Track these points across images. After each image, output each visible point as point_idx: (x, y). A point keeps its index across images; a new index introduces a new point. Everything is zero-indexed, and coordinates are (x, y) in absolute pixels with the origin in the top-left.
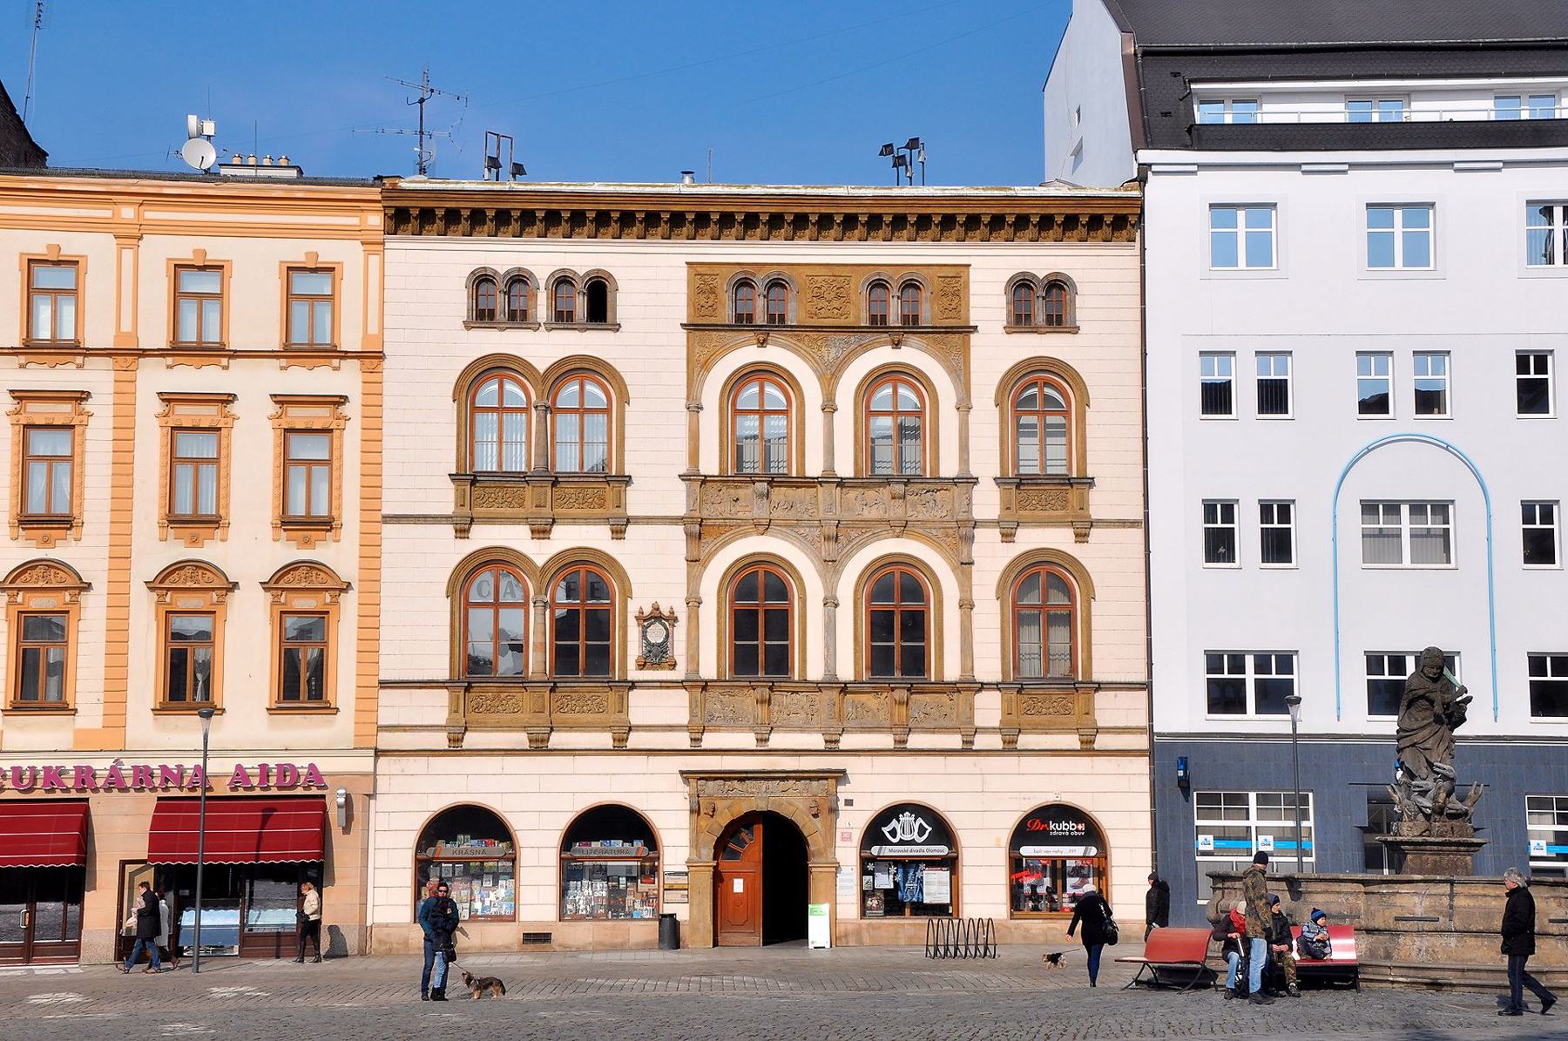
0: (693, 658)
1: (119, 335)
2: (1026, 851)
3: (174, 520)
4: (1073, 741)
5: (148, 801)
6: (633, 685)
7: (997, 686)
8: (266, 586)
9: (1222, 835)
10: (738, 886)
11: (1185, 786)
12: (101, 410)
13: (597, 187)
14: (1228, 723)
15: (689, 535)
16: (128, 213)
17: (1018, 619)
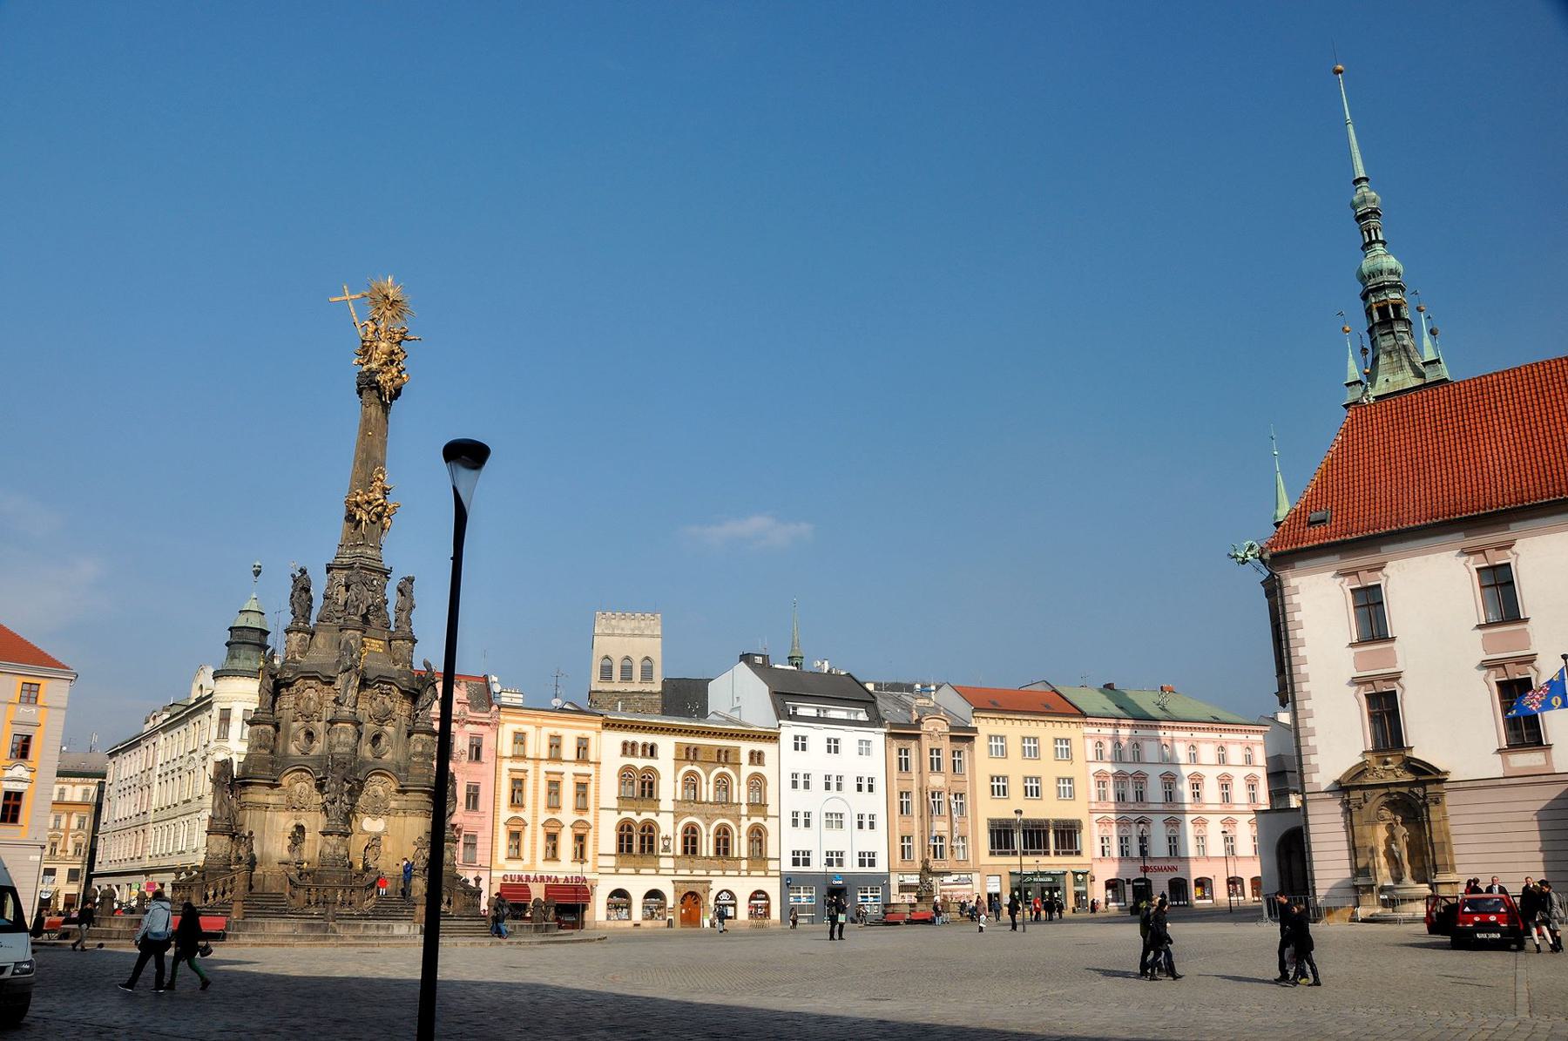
0: (675, 850)
1: (536, 754)
2: (753, 902)
3: (577, 809)
4: (762, 873)
5: (542, 886)
6: (661, 856)
7: (747, 859)
8: (571, 826)
9: (794, 897)
10: (684, 911)
11: (788, 884)
12: (530, 774)
13: (655, 721)
14: (796, 869)
15: (675, 816)
16: (539, 720)
17: (751, 840)
